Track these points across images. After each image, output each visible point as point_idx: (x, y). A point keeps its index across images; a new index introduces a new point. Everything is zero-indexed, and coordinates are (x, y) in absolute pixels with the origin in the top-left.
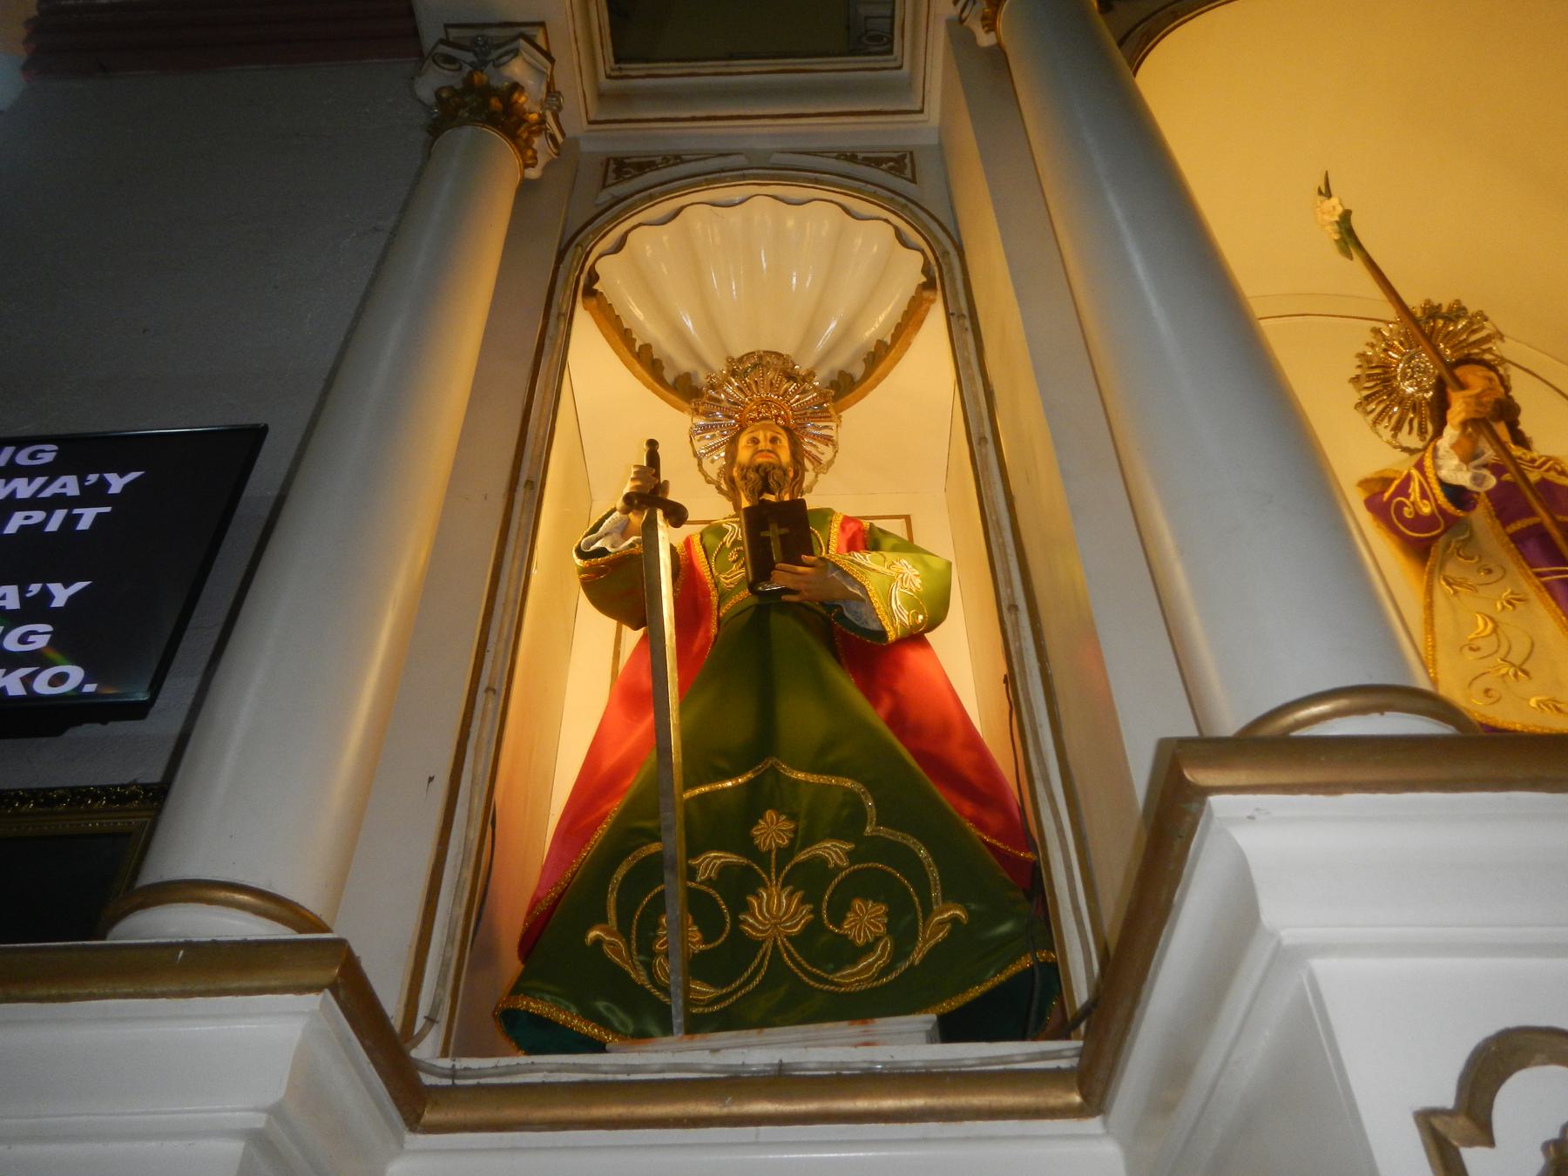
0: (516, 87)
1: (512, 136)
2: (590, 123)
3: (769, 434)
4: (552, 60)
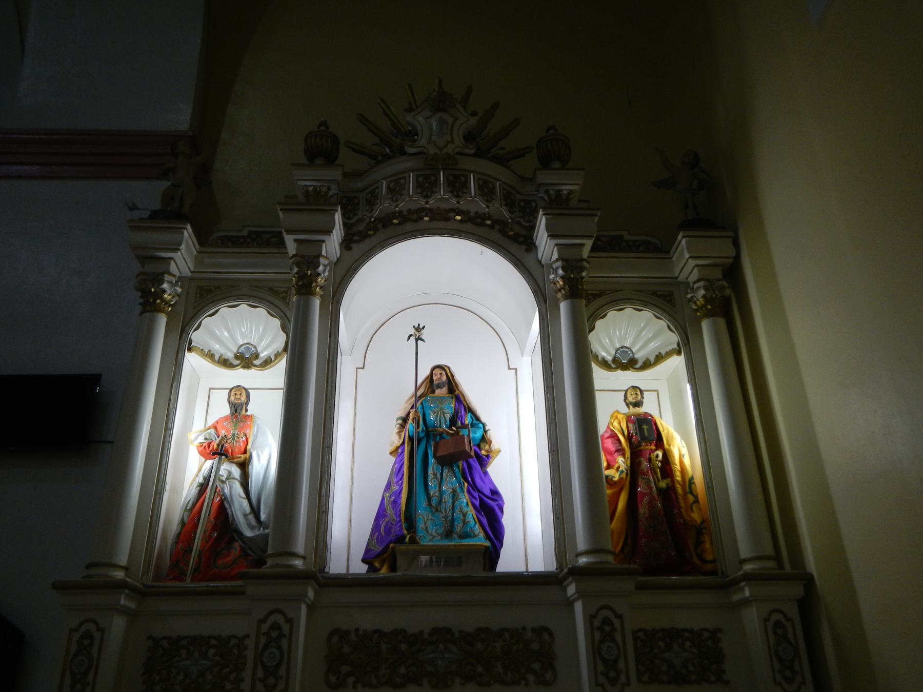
3: (239, 393)
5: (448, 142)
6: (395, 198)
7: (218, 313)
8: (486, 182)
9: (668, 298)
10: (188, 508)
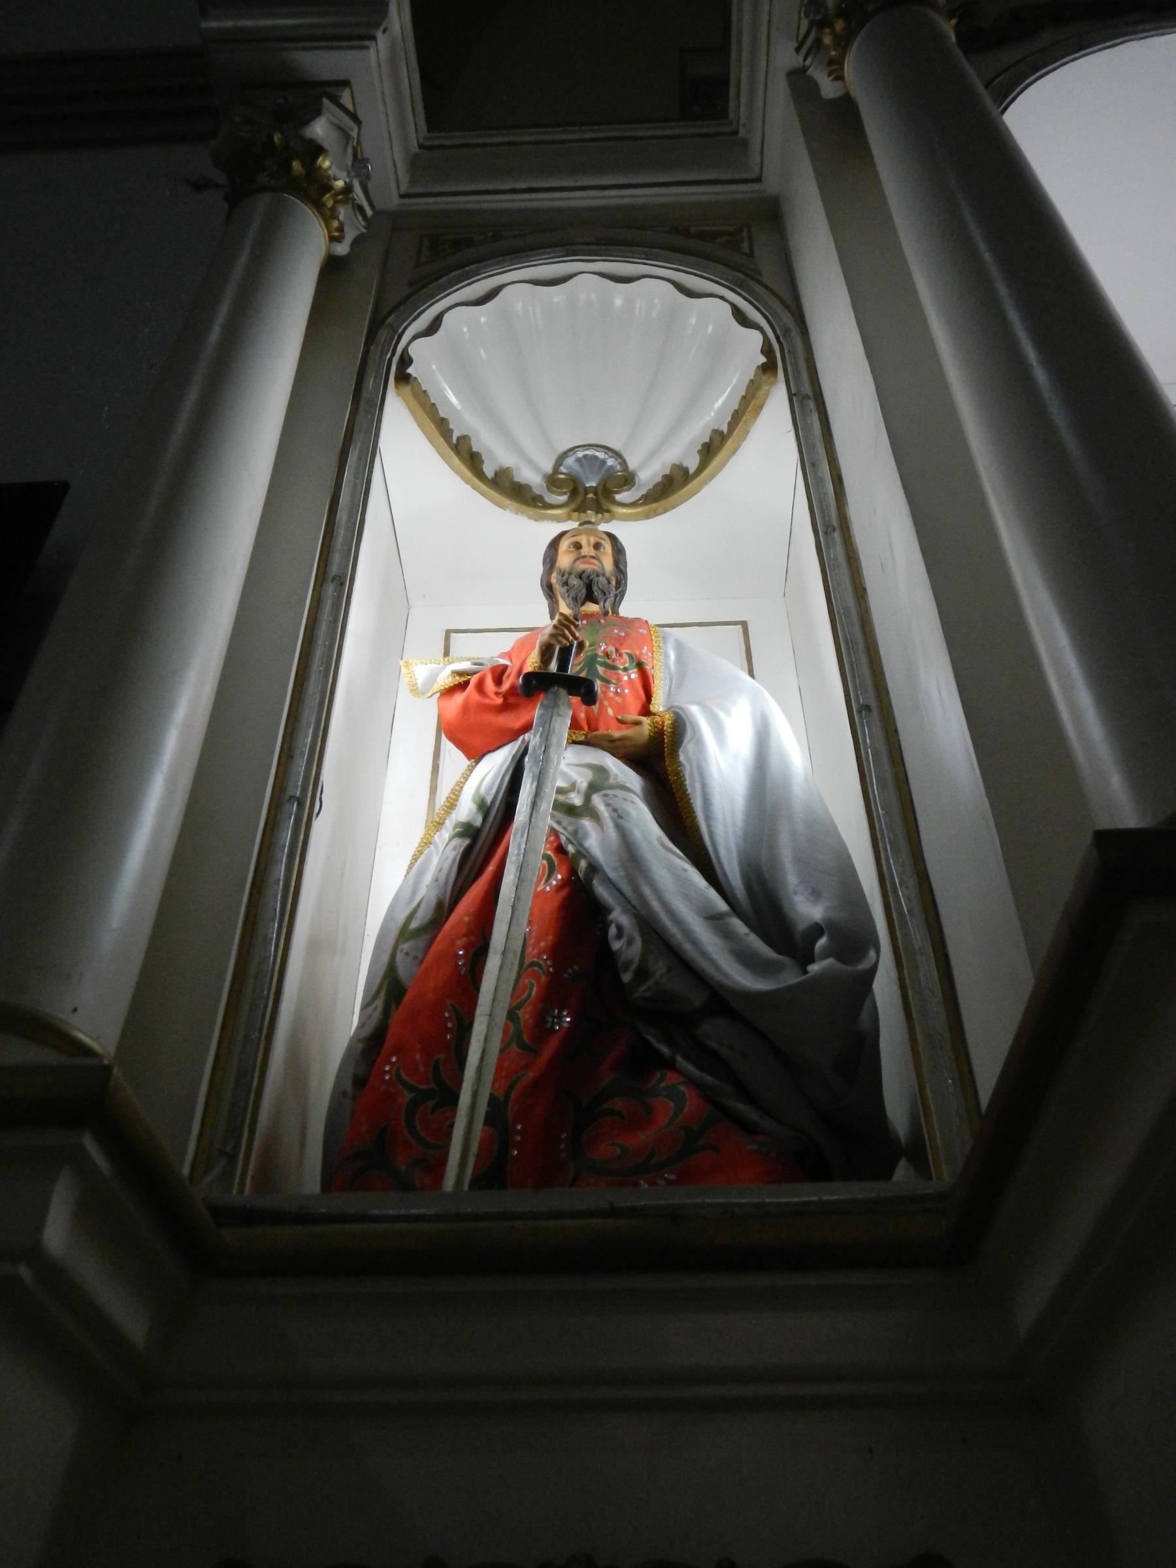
0: (317, 150)
1: (318, 205)
2: (403, 196)
4: (358, 122)
7: (497, 299)
10: (414, 924)
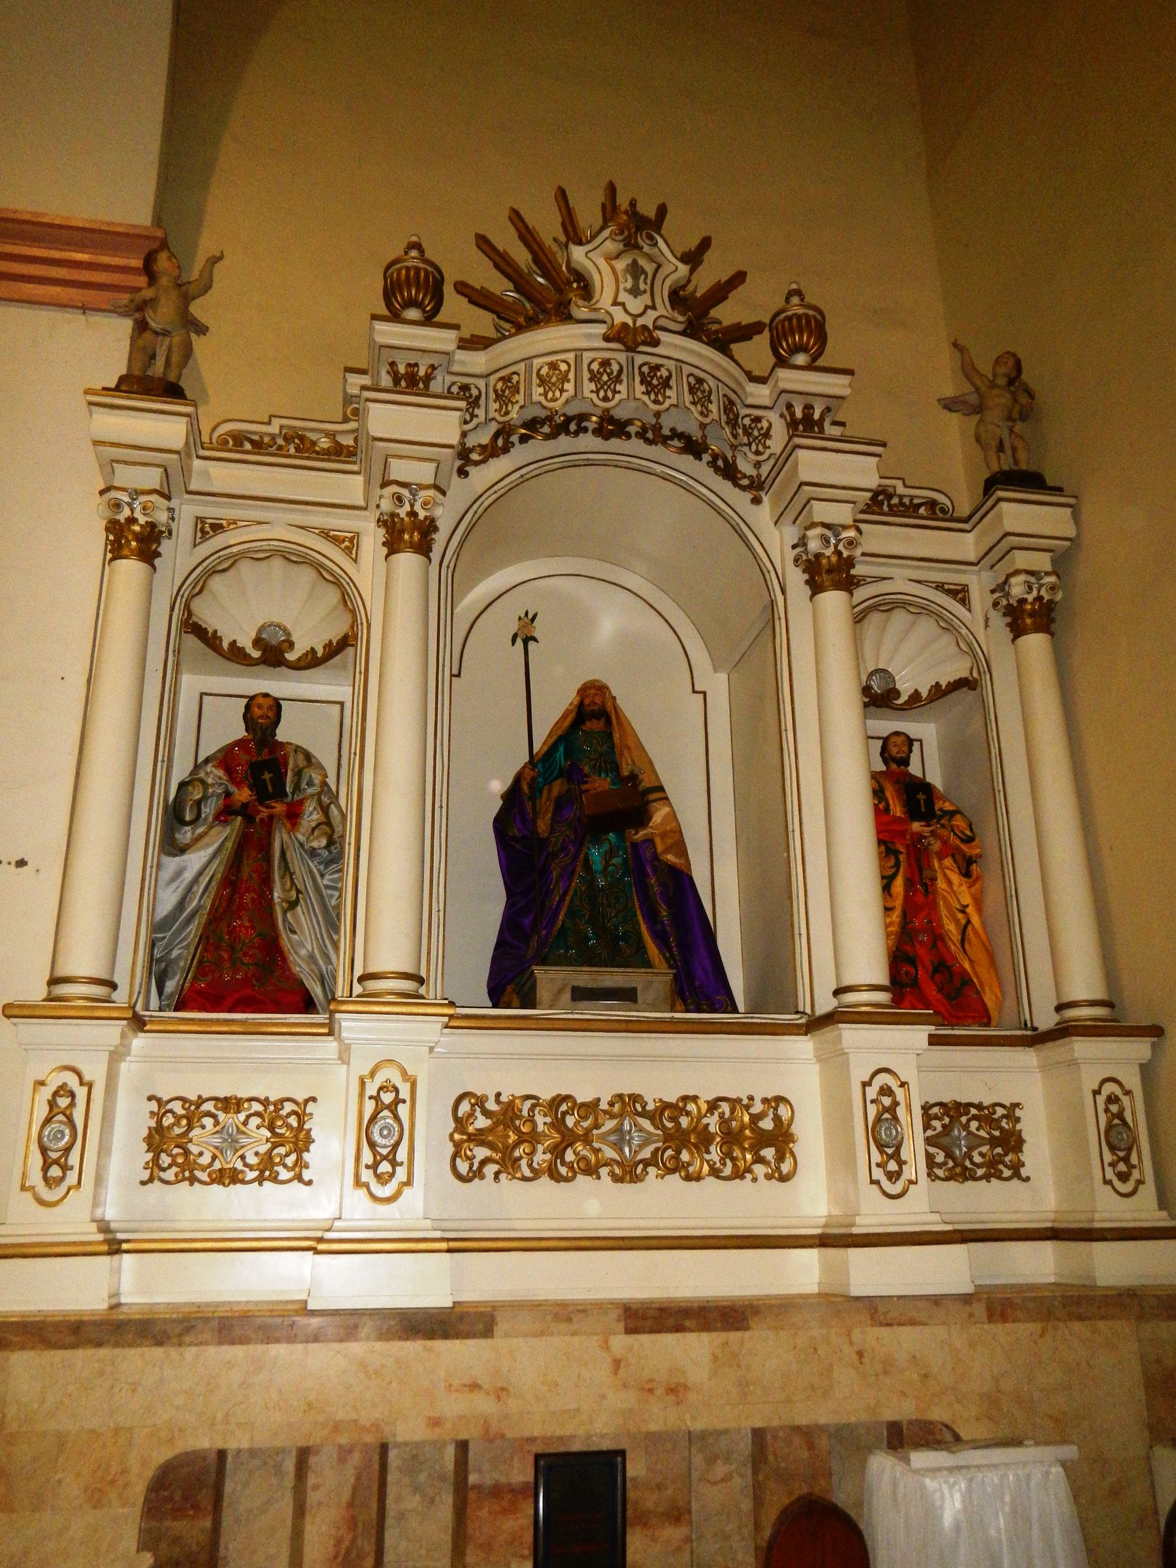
5: (647, 307)
6: (550, 395)
8: (700, 381)
9: (960, 596)
